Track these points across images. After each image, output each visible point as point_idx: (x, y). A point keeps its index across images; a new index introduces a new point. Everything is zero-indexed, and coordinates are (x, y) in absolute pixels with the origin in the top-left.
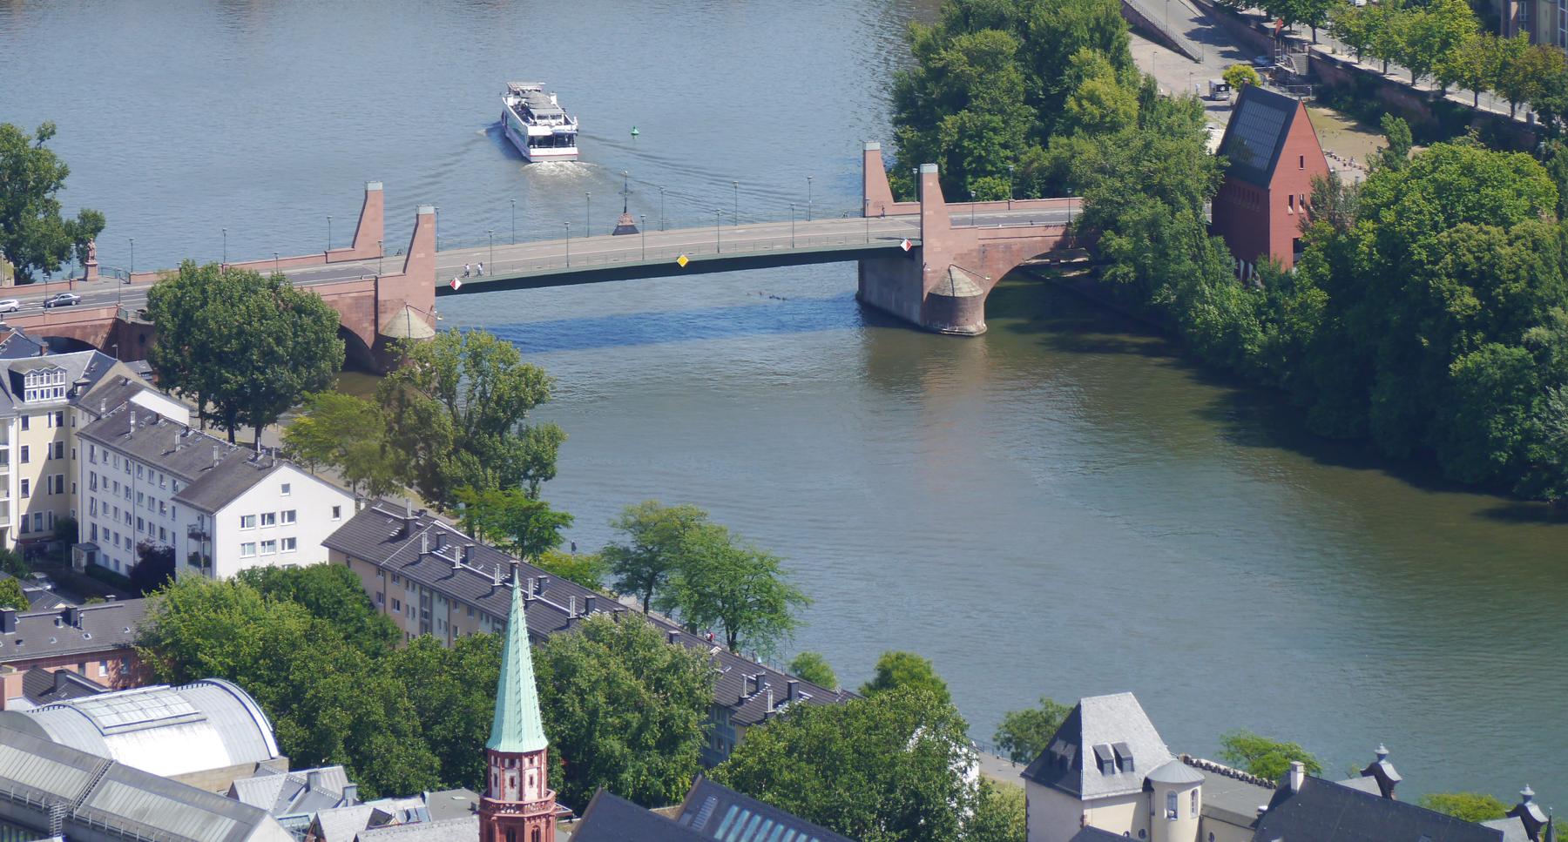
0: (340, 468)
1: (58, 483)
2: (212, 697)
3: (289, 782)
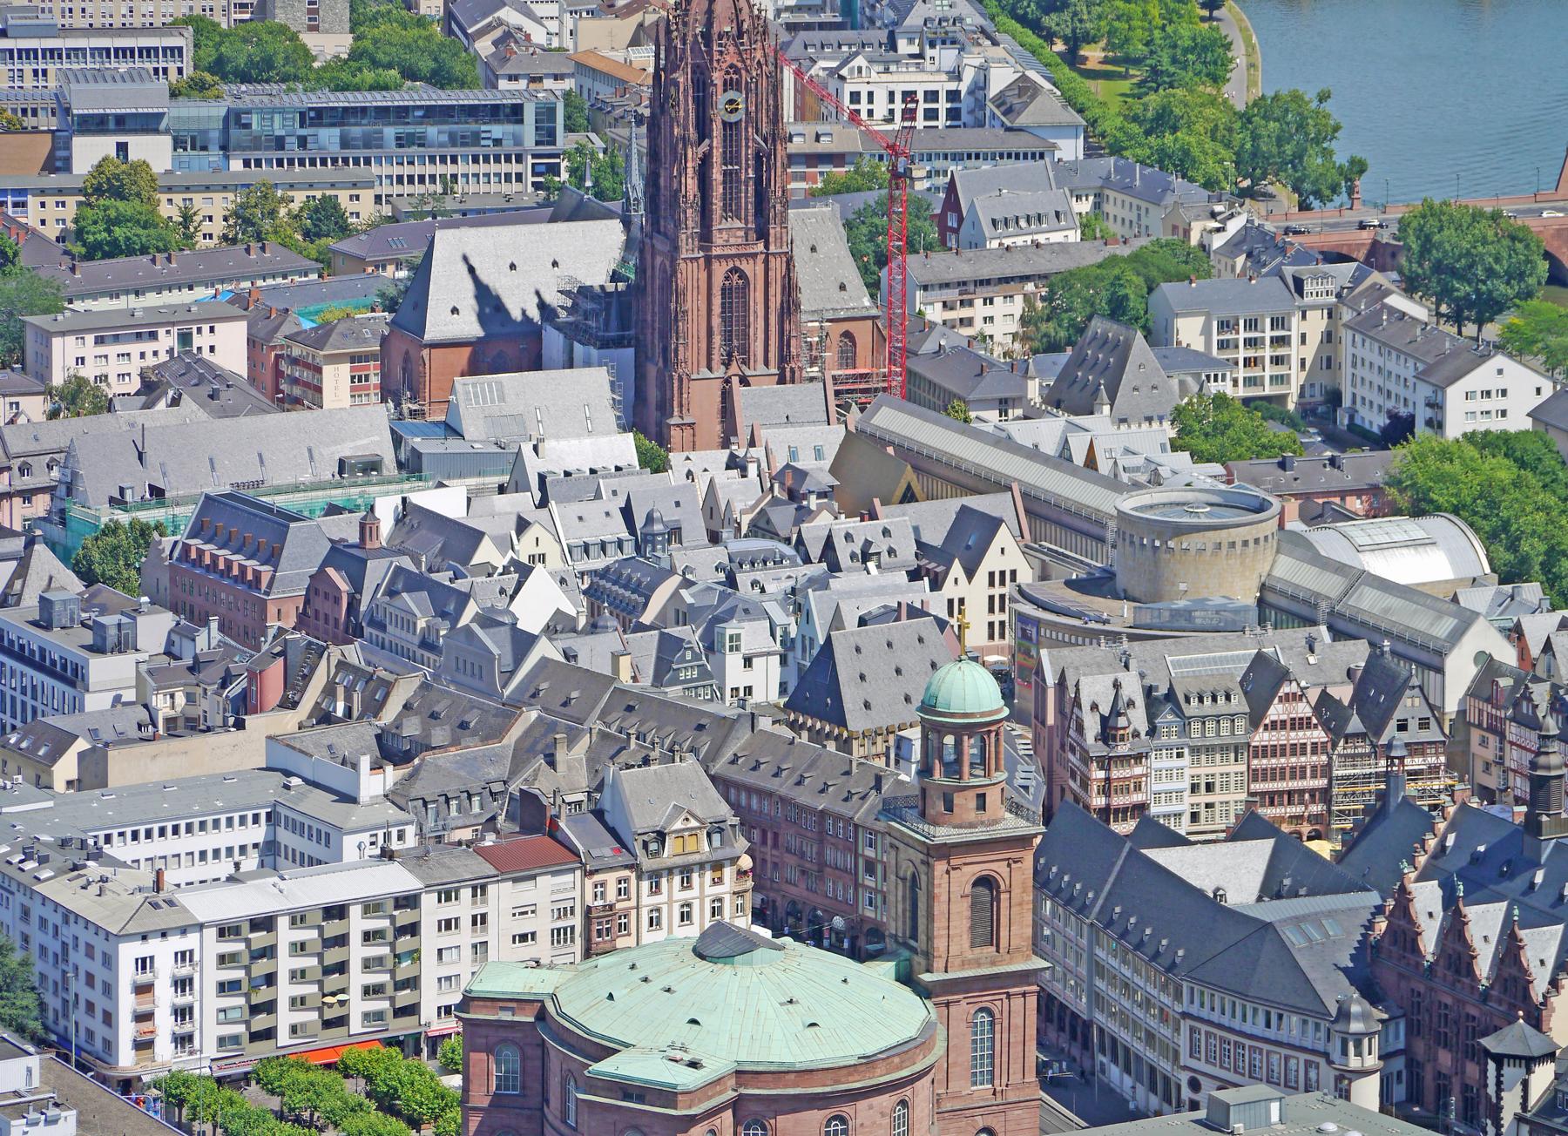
0: (1542, 358)
1: (1327, 362)
3: (1498, 593)
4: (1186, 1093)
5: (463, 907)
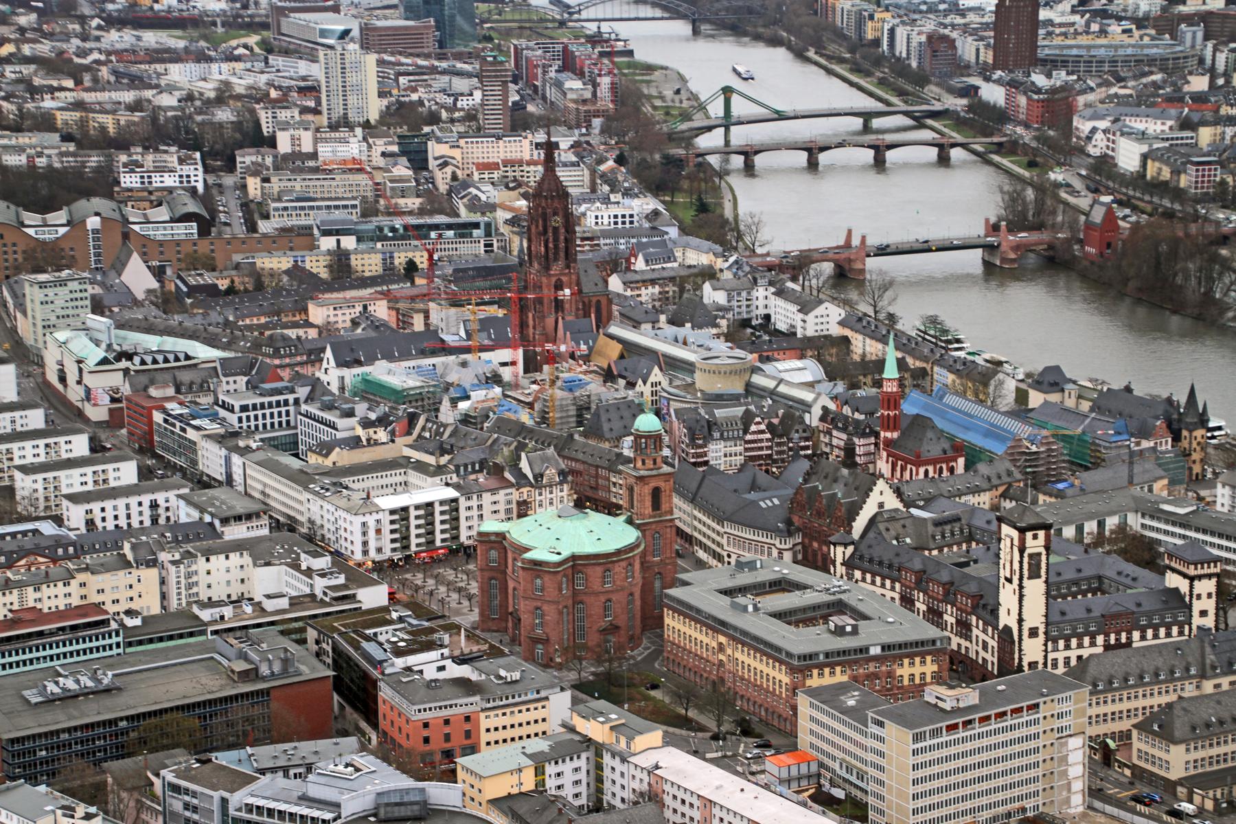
4: (726, 559)
5: (474, 503)
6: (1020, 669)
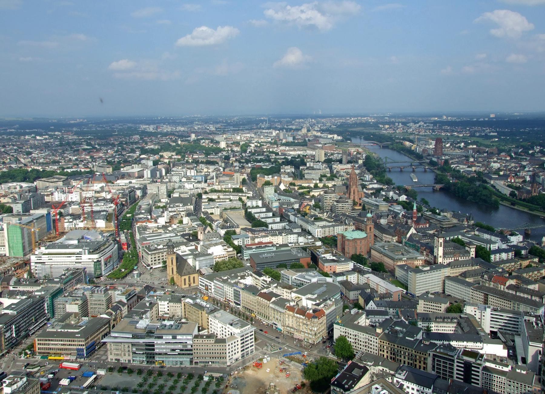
2: (400, 206)
6: (438, 263)
